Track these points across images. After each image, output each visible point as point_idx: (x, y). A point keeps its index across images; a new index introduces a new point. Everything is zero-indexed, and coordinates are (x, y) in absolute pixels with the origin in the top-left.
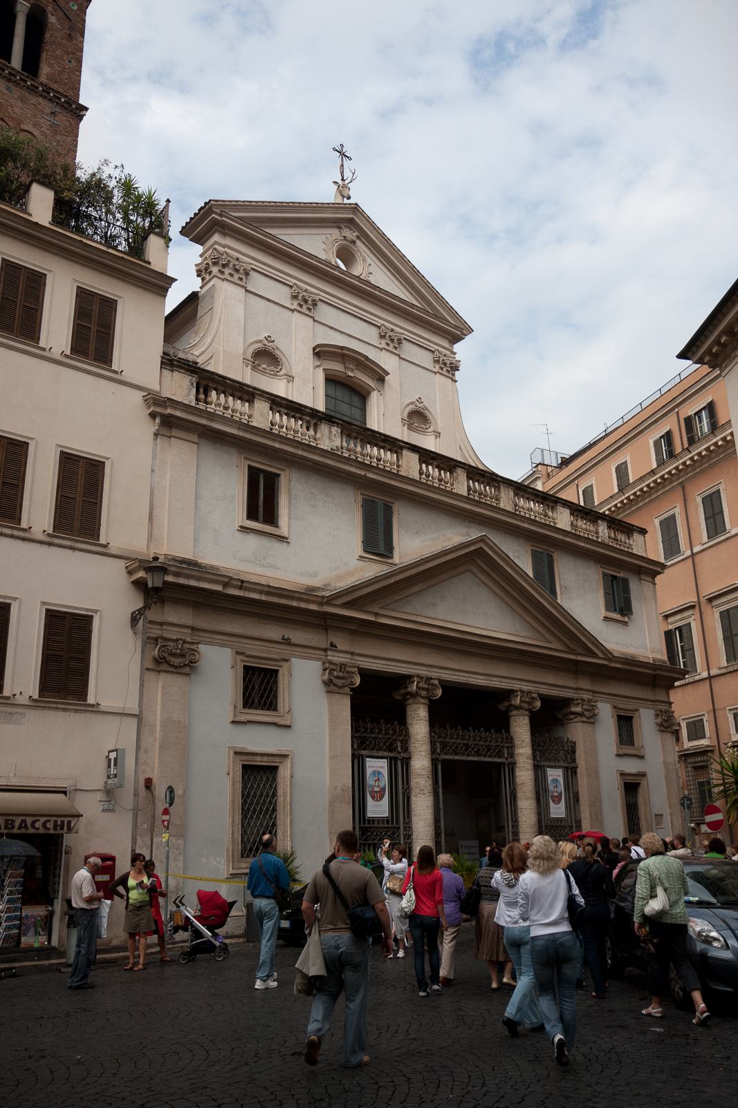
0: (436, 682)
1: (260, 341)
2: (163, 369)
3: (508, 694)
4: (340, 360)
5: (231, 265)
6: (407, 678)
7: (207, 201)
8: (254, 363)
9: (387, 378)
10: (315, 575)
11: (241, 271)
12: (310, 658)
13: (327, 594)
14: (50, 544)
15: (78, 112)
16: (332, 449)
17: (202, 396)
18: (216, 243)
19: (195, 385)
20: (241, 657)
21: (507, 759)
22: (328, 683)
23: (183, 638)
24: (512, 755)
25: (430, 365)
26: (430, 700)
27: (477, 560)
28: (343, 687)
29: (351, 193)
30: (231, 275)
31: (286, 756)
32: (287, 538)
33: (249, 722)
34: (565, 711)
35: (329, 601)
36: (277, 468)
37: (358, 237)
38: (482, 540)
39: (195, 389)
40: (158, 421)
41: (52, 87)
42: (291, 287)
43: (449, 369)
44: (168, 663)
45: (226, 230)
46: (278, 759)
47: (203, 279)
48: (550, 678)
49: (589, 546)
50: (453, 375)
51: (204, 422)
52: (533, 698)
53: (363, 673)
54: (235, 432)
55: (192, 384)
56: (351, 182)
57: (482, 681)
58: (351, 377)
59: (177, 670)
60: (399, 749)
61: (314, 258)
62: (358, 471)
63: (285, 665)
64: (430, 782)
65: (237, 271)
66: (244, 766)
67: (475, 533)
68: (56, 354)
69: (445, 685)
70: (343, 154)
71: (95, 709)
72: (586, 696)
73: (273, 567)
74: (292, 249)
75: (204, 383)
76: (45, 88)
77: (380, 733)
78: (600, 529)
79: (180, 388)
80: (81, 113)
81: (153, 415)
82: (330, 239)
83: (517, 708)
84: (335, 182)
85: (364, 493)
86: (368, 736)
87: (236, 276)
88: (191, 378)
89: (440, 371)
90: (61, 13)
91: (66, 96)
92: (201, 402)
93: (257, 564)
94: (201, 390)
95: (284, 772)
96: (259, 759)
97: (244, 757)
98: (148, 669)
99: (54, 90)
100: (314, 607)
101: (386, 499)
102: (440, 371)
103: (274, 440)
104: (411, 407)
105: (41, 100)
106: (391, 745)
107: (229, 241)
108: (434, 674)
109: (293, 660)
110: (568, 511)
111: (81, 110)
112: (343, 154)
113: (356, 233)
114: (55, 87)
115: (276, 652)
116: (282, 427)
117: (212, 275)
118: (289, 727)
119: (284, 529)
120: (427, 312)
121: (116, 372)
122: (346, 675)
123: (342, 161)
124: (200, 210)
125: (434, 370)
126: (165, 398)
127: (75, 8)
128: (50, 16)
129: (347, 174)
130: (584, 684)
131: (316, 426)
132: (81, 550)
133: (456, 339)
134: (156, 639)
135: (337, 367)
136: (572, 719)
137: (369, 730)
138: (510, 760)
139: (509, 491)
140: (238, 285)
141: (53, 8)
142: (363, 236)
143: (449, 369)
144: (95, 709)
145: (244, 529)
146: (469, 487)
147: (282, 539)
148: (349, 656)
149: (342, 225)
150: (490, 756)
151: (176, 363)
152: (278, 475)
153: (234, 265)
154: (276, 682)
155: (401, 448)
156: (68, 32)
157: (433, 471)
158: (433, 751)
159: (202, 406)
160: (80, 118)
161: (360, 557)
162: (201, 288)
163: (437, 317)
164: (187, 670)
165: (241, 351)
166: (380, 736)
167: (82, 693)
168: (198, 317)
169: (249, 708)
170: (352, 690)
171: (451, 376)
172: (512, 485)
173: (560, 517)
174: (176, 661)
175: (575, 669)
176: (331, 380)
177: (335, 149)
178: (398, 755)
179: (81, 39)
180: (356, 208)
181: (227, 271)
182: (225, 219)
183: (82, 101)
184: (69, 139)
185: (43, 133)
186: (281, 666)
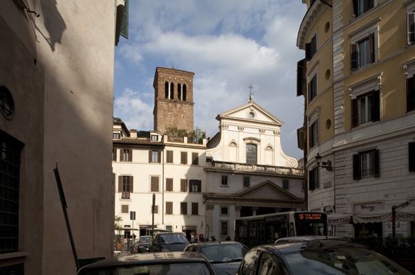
53: (243, 207)
69: (259, 208)
79: (208, 165)
107: (224, 121)
135: (249, 141)
175: (291, 202)
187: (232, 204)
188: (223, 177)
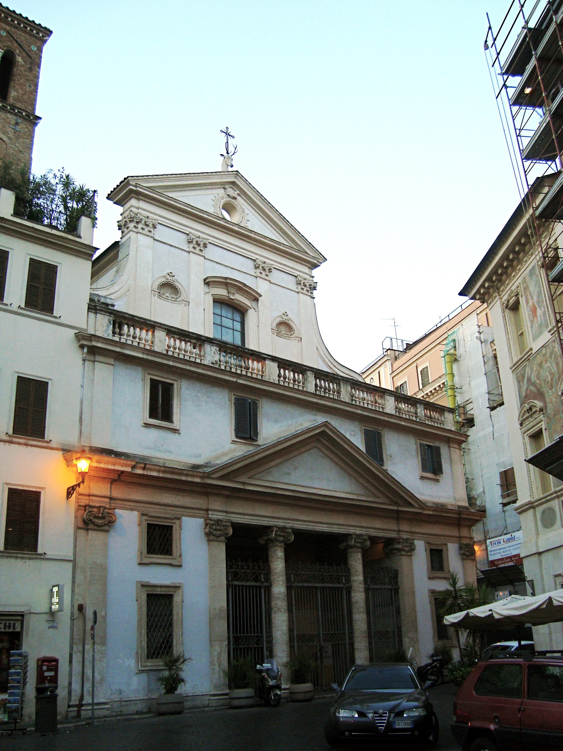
0: (290, 530)
1: (164, 277)
2: (89, 313)
3: (346, 536)
4: (225, 287)
5: (143, 222)
6: (268, 529)
7: (126, 177)
8: (159, 293)
9: (260, 299)
10: (199, 456)
11: (151, 225)
12: (196, 517)
13: (207, 470)
14: (11, 442)
15: (34, 121)
16: (212, 363)
17: (117, 330)
18: (132, 206)
19: (112, 322)
20: (145, 518)
21: (344, 584)
22: (208, 534)
23: (104, 505)
24: (348, 581)
25: (294, 287)
26: (286, 544)
27: (322, 439)
28: (220, 536)
29: (233, 163)
30: (143, 229)
31: (178, 587)
32: (178, 430)
33: (151, 563)
34: (390, 547)
35: (208, 475)
36: (171, 380)
37: (238, 195)
38: (326, 424)
39: (112, 326)
40: (85, 350)
41: (17, 106)
42: (188, 235)
43: (309, 289)
44: (93, 523)
45: (139, 195)
46: (172, 589)
47: (122, 232)
48: (378, 524)
49: (409, 425)
50: (312, 293)
51: (118, 350)
52: (365, 540)
53: (236, 526)
54: (140, 355)
55: (110, 322)
56: (234, 154)
57: (326, 529)
58: (233, 299)
59: (99, 528)
60: (263, 580)
61: (205, 213)
62: (231, 379)
63: (177, 522)
64: (285, 603)
65: (147, 225)
66: (148, 595)
67: (320, 419)
68: (15, 308)
69: (297, 533)
70: (228, 134)
71: (42, 557)
72: (405, 536)
73: (169, 451)
74: (188, 207)
75: (118, 320)
76: (12, 107)
77: (248, 569)
78: (419, 410)
80: (37, 122)
81: (82, 347)
82: (217, 197)
83: (352, 547)
84: (222, 155)
85: (236, 394)
86: (239, 571)
87: (147, 229)
88: (109, 317)
89: (302, 291)
90: (24, 54)
91: (26, 111)
92: (116, 334)
93: (157, 450)
94: (117, 326)
95: (177, 599)
96: (159, 589)
97: (148, 589)
98: (79, 528)
99: (18, 108)
100: (198, 480)
101: (254, 398)
102: (302, 291)
103: (169, 360)
104: (279, 319)
105: (9, 115)
106: (257, 577)
107: (142, 204)
108: (289, 524)
109: (184, 518)
110: (393, 398)
111: (37, 120)
112: (228, 134)
113: (238, 192)
114: (19, 105)
115: (170, 513)
116: (175, 349)
117: (129, 230)
118: (181, 566)
119: (176, 424)
120: (291, 248)
121: (55, 317)
122: (222, 528)
123: (227, 138)
124: (121, 183)
125: (297, 290)
126: (90, 334)
127: (35, 49)
128: (17, 56)
129: (231, 150)
130: (405, 527)
131: (200, 346)
132: (32, 446)
133: (315, 266)
134: (85, 506)
135: (222, 292)
136: (395, 553)
137: (240, 567)
138: (347, 585)
139: (347, 386)
140: (148, 236)
141: (19, 51)
142: (243, 193)
143: (309, 289)
144: (42, 557)
145: (147, 425)
146: (316, 385)
147: (175, 431)
148: (225, 514)
149: (226, 187)
150: (331, 583)
151: (98, 308)
152: (172, 384)
153: (145, 222)
154: (171, 535)
155: (265, 359)
156: (29, 66)
157: (290, 375)
158: (288, 580)
159: (116, 338)
160: (35, 124)
161: (233, 441)
162: (121, 238)
163: (299, 251)
164: (106, 528)
165: (150, 285)
166: (248, 571)
167: (34, 546)
168: (120, 258)
169: (152, 553)
170: (226, 538)
171: (310, 294)
172: (350, 382)
173: (387, 403)
174: (100, 522)
175: (398, 516)
176: (218, 301)
177: (222, 131)
178: (262, 584)
179: (38, 70)
180: (237, 174)
181: (140, 226)
182: (138, 189)
183: (37, 113)
184: (27, 141)
185: (9, 138)
186: (174, 523)
187: (192, 511)
188: (154, 385)
